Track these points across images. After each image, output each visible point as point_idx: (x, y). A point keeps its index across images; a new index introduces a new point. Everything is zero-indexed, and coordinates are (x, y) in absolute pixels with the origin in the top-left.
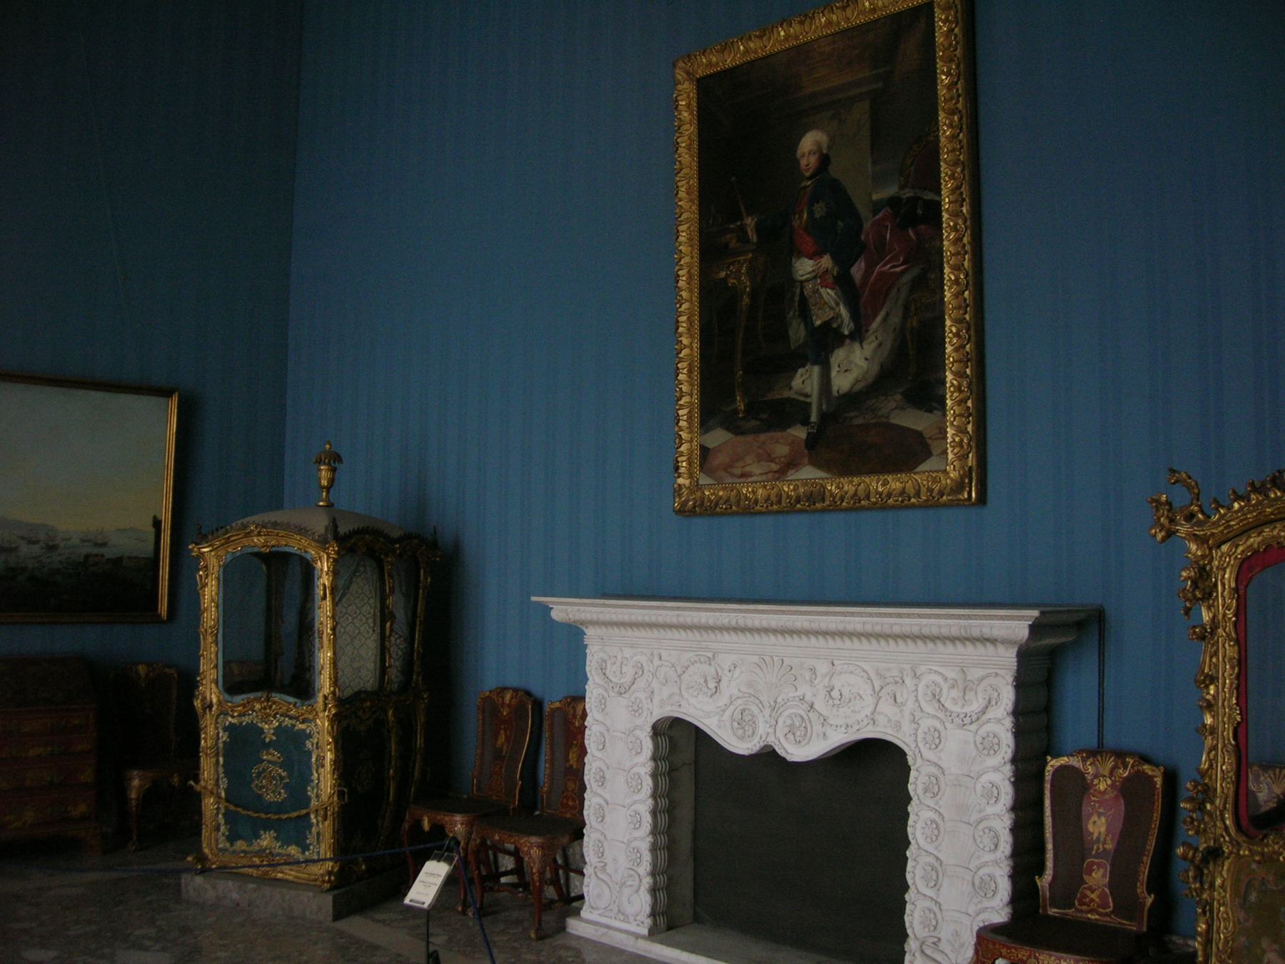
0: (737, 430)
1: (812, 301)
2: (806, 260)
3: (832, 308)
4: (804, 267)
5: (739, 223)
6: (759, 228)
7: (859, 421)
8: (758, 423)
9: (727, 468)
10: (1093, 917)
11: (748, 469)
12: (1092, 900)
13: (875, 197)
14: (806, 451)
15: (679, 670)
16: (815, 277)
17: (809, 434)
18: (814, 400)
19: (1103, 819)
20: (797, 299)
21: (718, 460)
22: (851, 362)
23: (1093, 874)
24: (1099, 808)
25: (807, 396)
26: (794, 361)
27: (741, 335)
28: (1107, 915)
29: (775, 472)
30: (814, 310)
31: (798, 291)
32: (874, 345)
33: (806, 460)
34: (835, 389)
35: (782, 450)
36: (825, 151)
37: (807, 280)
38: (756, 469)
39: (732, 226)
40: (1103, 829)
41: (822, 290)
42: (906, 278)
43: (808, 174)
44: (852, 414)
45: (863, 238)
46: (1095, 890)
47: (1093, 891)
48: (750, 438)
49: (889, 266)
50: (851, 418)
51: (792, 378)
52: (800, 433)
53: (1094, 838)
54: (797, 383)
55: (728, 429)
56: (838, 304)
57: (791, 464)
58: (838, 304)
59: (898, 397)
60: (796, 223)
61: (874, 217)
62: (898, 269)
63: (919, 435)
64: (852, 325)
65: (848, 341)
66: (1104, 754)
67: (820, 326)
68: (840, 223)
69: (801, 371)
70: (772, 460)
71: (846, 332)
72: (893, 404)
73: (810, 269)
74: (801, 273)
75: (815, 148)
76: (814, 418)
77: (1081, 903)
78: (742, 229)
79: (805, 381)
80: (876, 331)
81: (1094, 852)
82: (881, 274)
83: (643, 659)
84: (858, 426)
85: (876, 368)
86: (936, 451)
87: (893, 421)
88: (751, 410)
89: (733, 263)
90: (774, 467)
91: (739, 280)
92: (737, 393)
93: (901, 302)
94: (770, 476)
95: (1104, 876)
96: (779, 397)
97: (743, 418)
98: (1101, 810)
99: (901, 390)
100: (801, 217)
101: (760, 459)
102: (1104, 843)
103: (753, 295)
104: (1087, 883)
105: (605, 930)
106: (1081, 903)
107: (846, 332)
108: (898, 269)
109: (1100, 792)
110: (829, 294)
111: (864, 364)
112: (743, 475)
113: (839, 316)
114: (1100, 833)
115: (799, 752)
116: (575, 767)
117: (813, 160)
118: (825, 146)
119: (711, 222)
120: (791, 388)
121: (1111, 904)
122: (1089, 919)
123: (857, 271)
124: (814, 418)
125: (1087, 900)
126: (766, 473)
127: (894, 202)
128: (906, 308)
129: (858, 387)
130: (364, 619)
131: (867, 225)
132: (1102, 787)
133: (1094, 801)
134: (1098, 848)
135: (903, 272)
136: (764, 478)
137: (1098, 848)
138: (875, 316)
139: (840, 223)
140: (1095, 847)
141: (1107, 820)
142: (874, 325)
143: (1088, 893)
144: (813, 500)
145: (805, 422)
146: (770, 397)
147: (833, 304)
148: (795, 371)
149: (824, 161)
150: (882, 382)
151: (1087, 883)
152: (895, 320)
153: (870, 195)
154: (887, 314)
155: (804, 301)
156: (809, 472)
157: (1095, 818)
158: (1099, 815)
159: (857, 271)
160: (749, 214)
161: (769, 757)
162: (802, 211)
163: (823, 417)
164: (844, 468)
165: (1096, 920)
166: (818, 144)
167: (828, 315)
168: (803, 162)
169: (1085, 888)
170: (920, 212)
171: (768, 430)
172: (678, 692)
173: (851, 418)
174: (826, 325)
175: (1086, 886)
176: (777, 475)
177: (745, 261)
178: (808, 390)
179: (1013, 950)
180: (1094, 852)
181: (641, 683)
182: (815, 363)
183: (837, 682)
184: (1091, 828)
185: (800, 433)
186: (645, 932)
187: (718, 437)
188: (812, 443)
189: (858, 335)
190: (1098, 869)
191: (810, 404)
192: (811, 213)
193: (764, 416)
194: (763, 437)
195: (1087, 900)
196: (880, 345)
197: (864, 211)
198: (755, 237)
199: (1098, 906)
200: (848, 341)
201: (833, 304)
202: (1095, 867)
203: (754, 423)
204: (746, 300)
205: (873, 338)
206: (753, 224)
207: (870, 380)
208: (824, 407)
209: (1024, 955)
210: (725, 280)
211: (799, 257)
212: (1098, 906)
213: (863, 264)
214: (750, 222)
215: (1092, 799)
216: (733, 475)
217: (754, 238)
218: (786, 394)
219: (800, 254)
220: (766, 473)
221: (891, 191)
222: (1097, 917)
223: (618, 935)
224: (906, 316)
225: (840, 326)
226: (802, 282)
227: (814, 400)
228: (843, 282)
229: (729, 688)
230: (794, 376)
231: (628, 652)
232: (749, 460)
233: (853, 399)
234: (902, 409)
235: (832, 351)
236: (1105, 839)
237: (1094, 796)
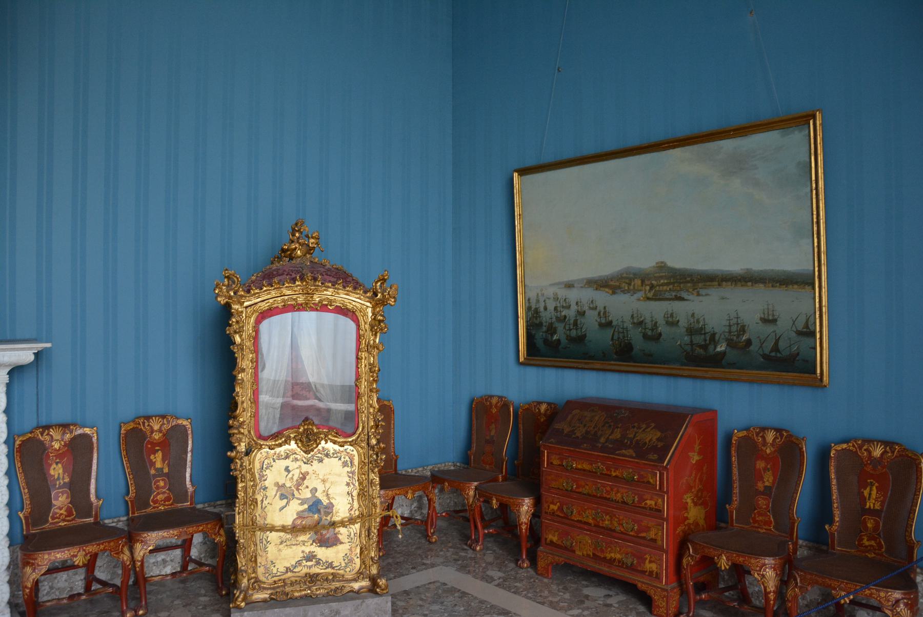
10: (63, 524)
12: (61, 514)
19: (60, 465)
23: (60, 499)
24: (56, 459)
28: (73, 520)
40: (61, 471)
46: (62, 508)
47: (61, 509)
53: (56, 478)
66: (54, 427)
77: (53, 518)
81: (57, 486)
95: (67, 498)
98: (58, 460)
102: (63, 479)
104: (56, 506)
106: (53, 518)
109: (56, 450)
114: (59, 474)
121: (74, 513)
122: (60, 526)
125: (58, 515)
132: (56, 446)
133: (52, 456)
134: (60, 483)
137: (60, 483)
140: (58, 483)
141: (62, 466)
143: (57, 511)
151: (56, 506)
157: (54, 466)
158: (57, 463)
165: (65, 525)
169: (55, 509)
175: (55, 507)
179: (66, 552)
180: (57, 486)
184: (52, 472)
190: (63, 494)
195: (58, 515)
199: (66, 516)
202: (60, 494)
209: (74, 552)
212: (66, 516)
215: (51, 455)
222: (65, 523)
236: (63, 477)
237: (52, 453)
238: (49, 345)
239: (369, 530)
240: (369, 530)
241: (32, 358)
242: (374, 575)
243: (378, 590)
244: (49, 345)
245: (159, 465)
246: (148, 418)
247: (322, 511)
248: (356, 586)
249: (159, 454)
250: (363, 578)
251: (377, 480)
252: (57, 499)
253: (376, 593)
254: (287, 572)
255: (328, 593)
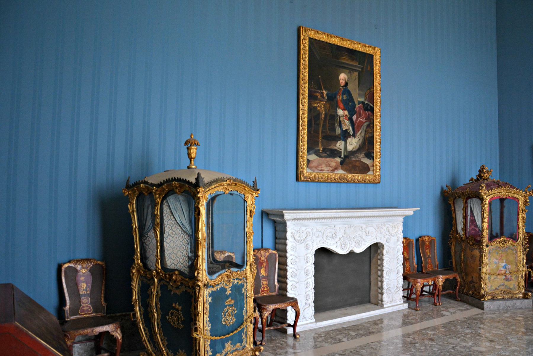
0: (320, 156)
1: (342, 123)
2: (341, 110)
3: (348, 126)
4: (340, 112)
5: (321, 91)
6: (327, 95)
7: (354, 159)
8: (326, 155)
9: (316, 167)
11: (323, 168)
13: (359, 100)
14: (340, 165)
15: (323, 232)
16: (343, 116)
17: (341, 160)
18: (343, 151)
20: (338, 121)
21: (312, 164)
22: (352, 142)
25: (340, 149)
26: (336, 139)
27: (321, 126)
29: (331, 170)
30: (343, 125)
31: (339, 118)
32: (358, 139)
33: (340, 168)
34: (348, 149)
35: (333, 164)
36: (347, 81)
37: (341, 116)
38: (326, 169)
39: (319, 91)
41: (345, 120)
42: (366, 124)
43: (342, 85)
44: (352, 157)
45: (356, 109)
47: (407, 267)
48: (324, 159)
49: (362, 119)
50: (352, 158)
51: (336, 143)
52: (339, 160)
54: (338, 145)
55: (316, 155)
56: (349, 126)
57: (336, 169)
58: (349, 126)
59: (363, 154)
60: (338, 98)
61: (359, 104)
62: (364, 121)
63: (367, 165)
64: (353, 132)
65: (351, 137)
67: (345, 130)
68: (350, 103)
69: (339, 142)
70: (330, 167)
71: (351, 134)
72: (362, 156)
73: (342, 113)
74: (339, 113)
75: (344, 79)
76: (342, 156)
78: (322, 93)
79: (340, 145)
80: (358, 136)
82: (360, 121)
83: (310, 231)
84: (354, 160)
85: (358, 146)
86: (371, 170)
87: (362, 160)
88: (324, 150)
89: (319, 103)
90: (331, 169)
91: (321, 109)
92: (320, 144)
93: (364, 130)
94: (330, 171)
96: (332, 148)
97: (321, 153)
99: (364, 153)
100: (340, 97)
101: (327, 166)
103: (326, 115)
105: (304, 326)
107: (351, 134)
108: (364, 121)
110: (347, 122)
111: (355, 144)
112: (321, 170)
113: (349, 129)
115: (359, 250)
116: (264, 275)
117: (344, 82)
118: (347, 79)
119: (312, 87)
120: (336, 146)
123: (354, 118)
124: (342, 156)
126: (329, 170)
127: (363, 103)
128: (366, 131)
129: (354, 150)
130: (170, 227)
131: (357, 106)
135: (365, 122)
136: (328, 172)
138: (359, 131)
139: (350, 103)
142: (358, 134)
144: (342, 180)
145: (340, 157)
146: (330, 148)
147: (348, 125)
148: (338, 141)
149: (346, 84)
150: (360, 149)
152: (363, 134)
153: (358, 98)
154: (361, 132)
155: (340, 122)
156: (341, 172)
159: (354, 118)
160: (325, 89)
161: (351, 253)
162: (340, 95)
163: (346, 157)
164: (350, 171)
166: (345, 78)
167: (347, 128)
168: (341, 81)
170: (369, 108)
171: (329, 158)
172: (322, 239)
173: (352, 158)
174: (346, 130)
176: (332, 171)
177: (323, 104)
178: (341, 148)
181: (309, 238)
182: (343, 140)
183: (368, 230)
185: (339, 160)
186: (314, 320)
187: (313, 157)
188: (342, 163)
189: (354, 135)
191: (341, 152)
192: (343, 97)
193: (328, 153)
194: (328, 159)
196: (359, 140)
197: (356, 103)
198: (326, 97)
200: (351, 137)
201: (348, 125)
203: (325, 155)
204: (323, 116)
205: (358, 137)
206: (326, 93)
207: (357, 148)
208: (345, 153)
210: (316, 107)
211: (339, 109)
213: (356, 117)
214: (325, 92)
216: (318, 170)
217: (326, 98)
218: (335, 148)
219: (339, 108)
220: (329, 170)
221: (362, 100)
223: (309, 325)
224: (365, 134)
225: (350, 132)
226: (340, 116)
227: (343, 151)
228: (350, 119)
229: (339, 235)
230: (337, 143)
231: (303, 229)
232: (323, 165)
233: (353, 153)
234: (364, 158)
235: (348, 138)
238: (419, 209)
239: (522, 276)
240: (522, 276)
241: (413, 213)
242: (524, 292)
243: (528, 297)
244: (419, 209)
245: (428, 254)
246: (425, 236)
247: (507, 268)
248: (518, 296)
249: (428, 250)
250: (520, 293)
251: (525, 258)
252: (406, 264)
253: (527, 298)
254: (495, 290)
255: (509, 298)
